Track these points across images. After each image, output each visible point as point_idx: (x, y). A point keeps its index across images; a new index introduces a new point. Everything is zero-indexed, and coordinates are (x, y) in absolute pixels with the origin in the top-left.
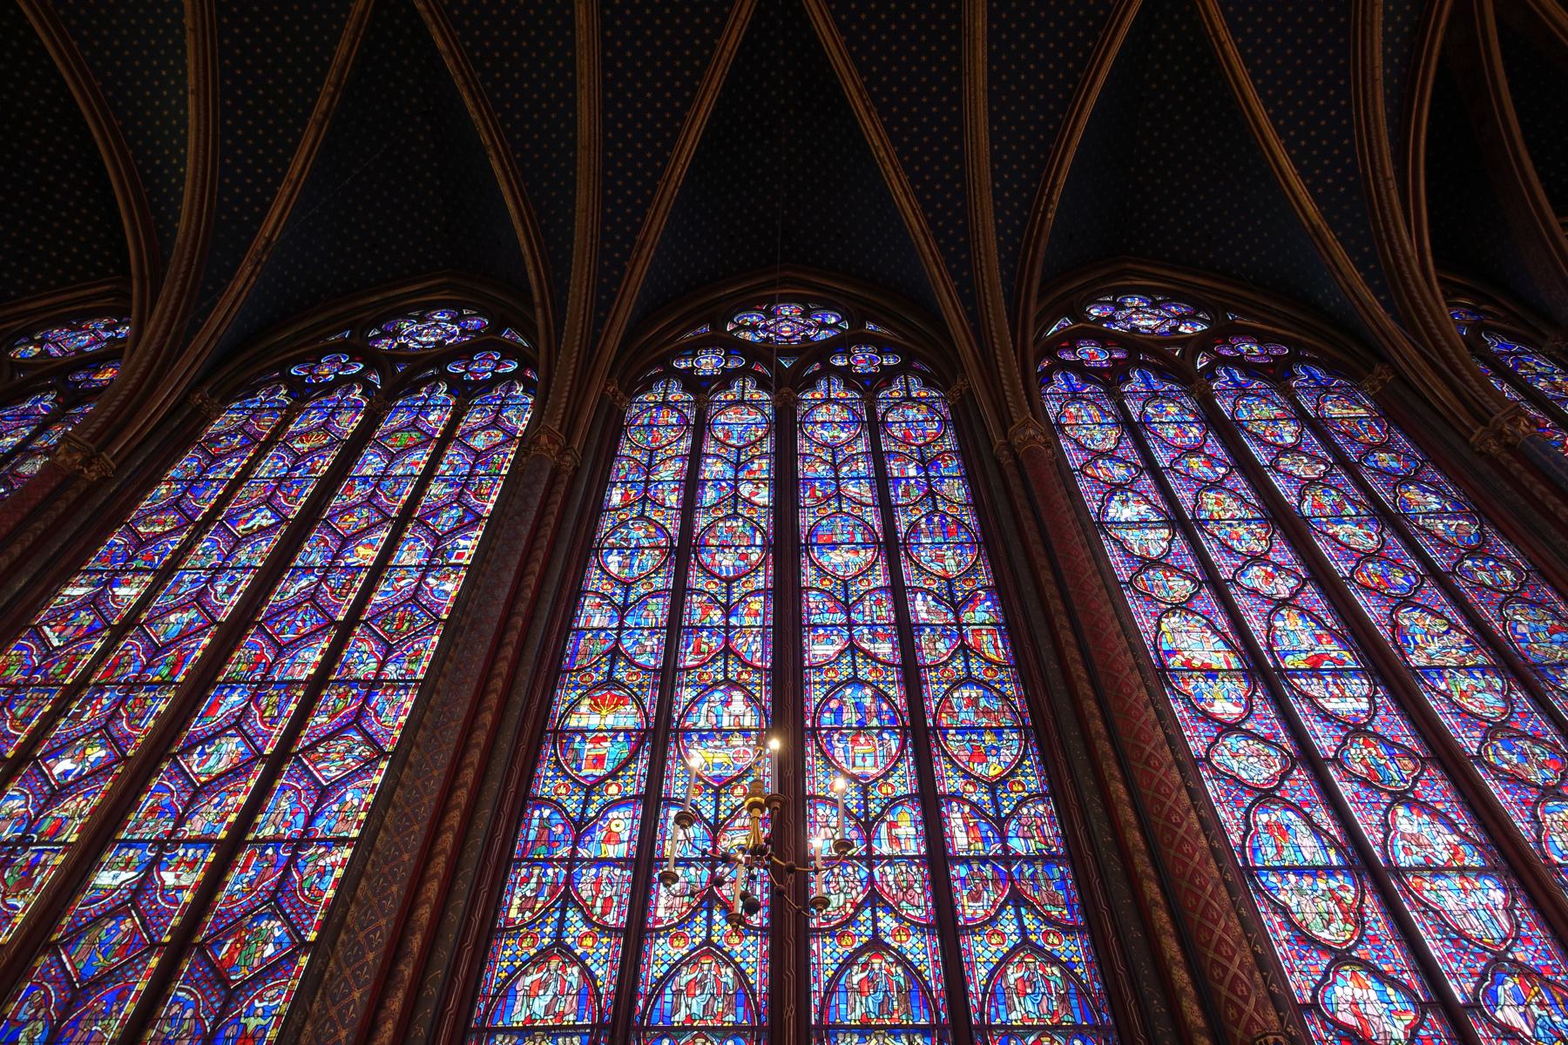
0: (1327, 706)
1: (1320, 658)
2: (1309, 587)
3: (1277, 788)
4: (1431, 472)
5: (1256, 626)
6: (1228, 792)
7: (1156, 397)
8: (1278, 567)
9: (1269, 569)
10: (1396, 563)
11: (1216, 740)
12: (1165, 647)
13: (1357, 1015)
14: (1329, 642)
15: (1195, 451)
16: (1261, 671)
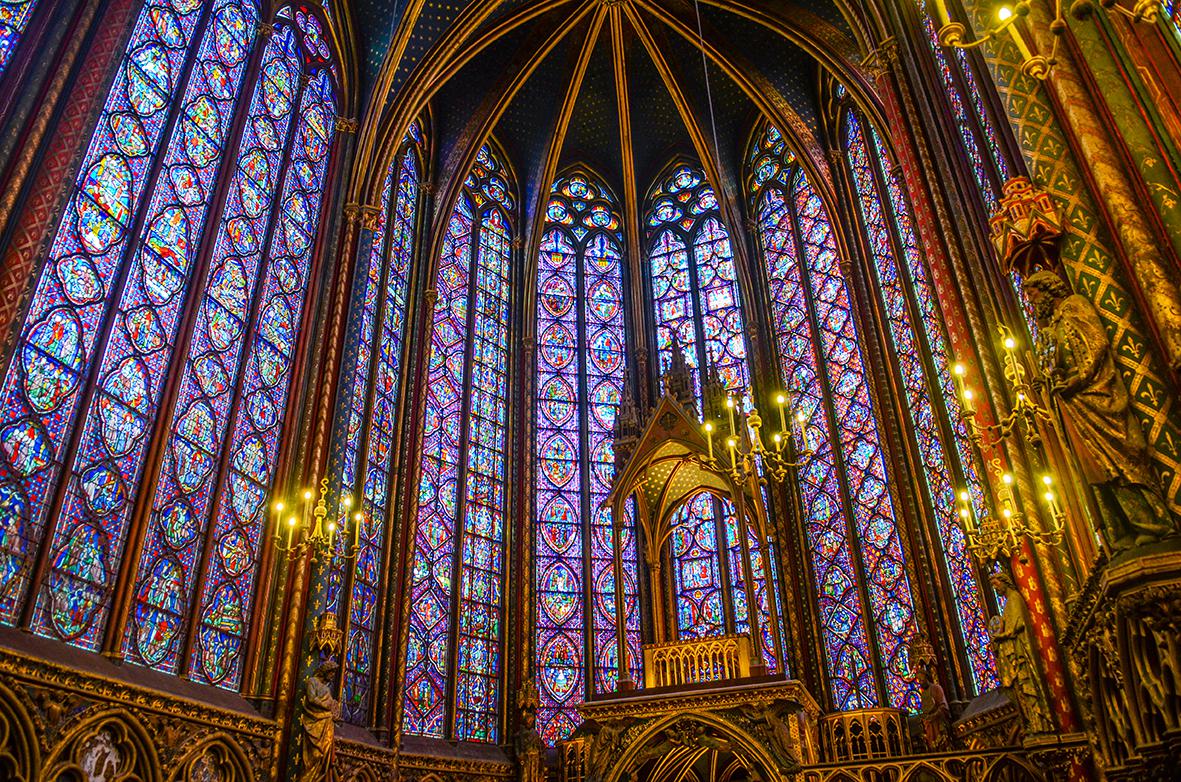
0: (149, 282)
1: (170, 253)
2: (202, 208)
3: (80, 307)
4: (315, 201)
5: (155, 206)
6: (50, 290)
7: (239, 7)
8: (198, 182)
9: (193, 180)
10: (253, 233)
11: (71, 256)
12: (93, 176)
13: (16, 449)
14: (182, 248)
15: (225, 68)
16: (133, 234)
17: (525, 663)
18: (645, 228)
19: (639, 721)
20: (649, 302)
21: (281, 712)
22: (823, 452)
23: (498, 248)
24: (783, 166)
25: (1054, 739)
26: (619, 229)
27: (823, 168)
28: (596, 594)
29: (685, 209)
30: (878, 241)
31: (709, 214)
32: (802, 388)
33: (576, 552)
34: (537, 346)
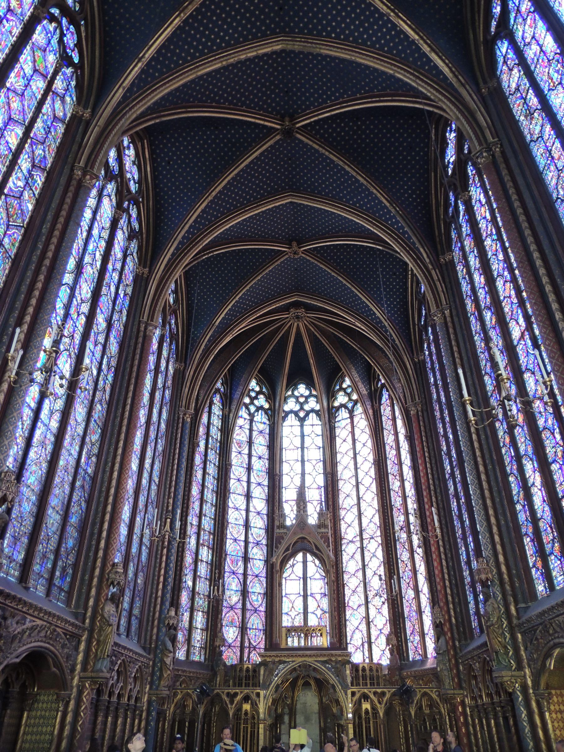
17: (219, 625)
18: (284, 411)
19: (285, 662)
20: (281, 449)
21: (152, 652)
22: (354, 540)
23: (217, 413)
24: (350, 399)
25: (452, 692)
26: (269, 409)
27: (371, 411)
28: (248, 592)
29: (302, 405)
30: (391, 454)
31: (312, 411)
32: (348, 508)
33: (241, 571)
34: (231, 465)
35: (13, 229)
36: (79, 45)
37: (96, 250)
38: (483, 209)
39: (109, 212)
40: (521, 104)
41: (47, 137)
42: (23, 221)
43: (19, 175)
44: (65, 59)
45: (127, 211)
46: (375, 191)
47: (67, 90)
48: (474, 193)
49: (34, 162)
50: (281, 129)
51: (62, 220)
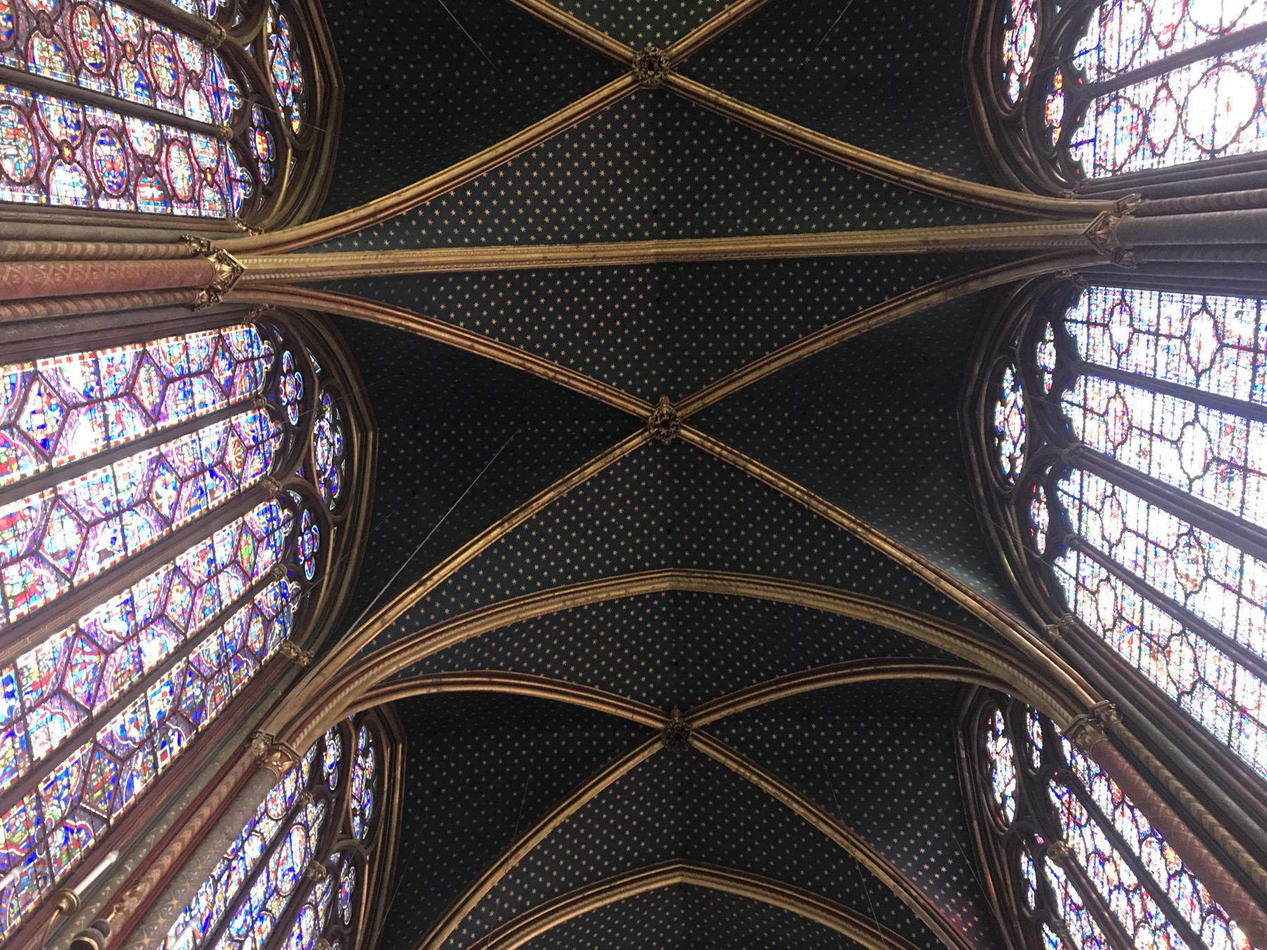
35: (81, 818)
36: (319, 557)
37: (246, 936)
38: (1109, 867)
39: (298, 861)
40: (1136, 639)
41: (220, 671)
42: (110, 811)
43: (142, 718)
44: (289, 562)
45: (334, 871)
46: (859, 856)
47: (279, 612)
48: (1077, 839)
49: (179, 704)
50: (665, 730)
51: (197, 823)
